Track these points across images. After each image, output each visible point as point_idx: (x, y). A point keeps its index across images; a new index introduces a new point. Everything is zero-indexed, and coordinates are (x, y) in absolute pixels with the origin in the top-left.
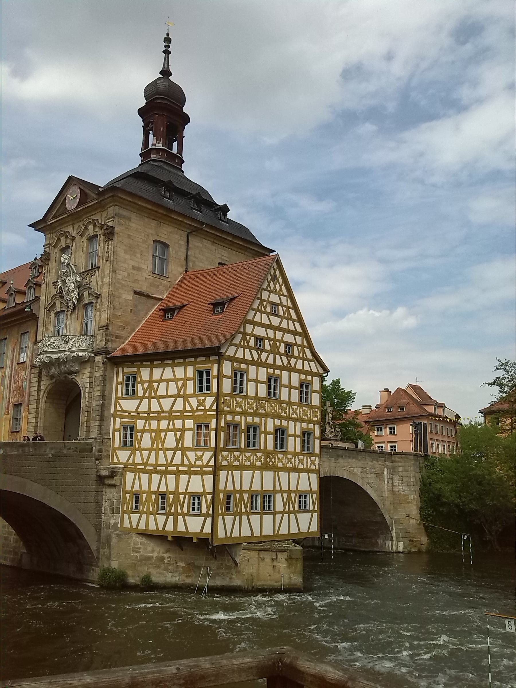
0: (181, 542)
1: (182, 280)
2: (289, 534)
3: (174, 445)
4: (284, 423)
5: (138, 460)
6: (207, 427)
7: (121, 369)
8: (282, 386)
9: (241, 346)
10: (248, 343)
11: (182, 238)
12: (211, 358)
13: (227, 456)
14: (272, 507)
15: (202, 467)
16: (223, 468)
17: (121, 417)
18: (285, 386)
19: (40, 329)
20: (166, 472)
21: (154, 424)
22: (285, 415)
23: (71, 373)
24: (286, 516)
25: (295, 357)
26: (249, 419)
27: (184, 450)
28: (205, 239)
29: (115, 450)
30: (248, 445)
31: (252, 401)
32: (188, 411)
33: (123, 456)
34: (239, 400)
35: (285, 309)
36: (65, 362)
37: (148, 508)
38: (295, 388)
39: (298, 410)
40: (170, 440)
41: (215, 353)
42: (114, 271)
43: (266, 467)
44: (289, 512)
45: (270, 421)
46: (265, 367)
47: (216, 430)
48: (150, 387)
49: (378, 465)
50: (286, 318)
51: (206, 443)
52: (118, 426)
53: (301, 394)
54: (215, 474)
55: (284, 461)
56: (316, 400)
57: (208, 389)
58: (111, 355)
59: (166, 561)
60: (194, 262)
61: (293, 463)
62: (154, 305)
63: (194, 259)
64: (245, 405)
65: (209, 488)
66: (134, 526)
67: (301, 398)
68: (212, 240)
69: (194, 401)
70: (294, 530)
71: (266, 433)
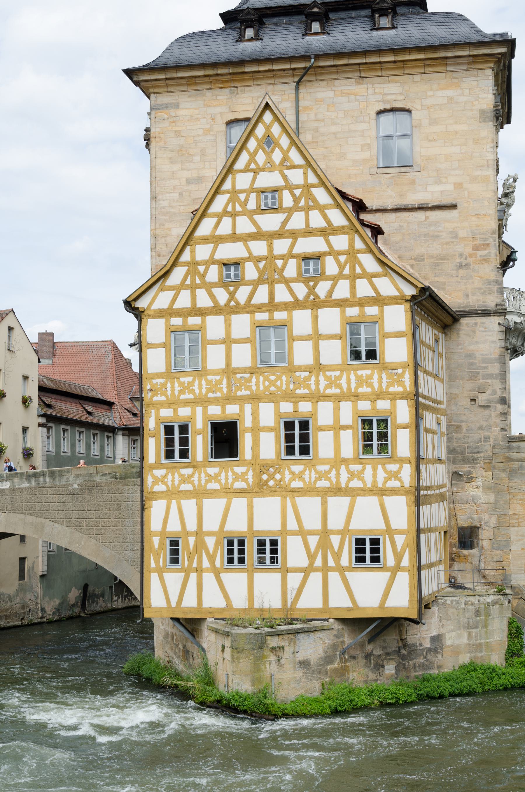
4: (305, 408)
8: (293, 339)
10: (203, 276)
11: (286, 97)
13: (166, 476)
16: (160, 495)
18: (302, 338)
22: (307, 391)
28: (338, 79)
31: (218, 377)
34: (186, 380)
35: (297, 192)
39: (344, 378)
43: (261, 488)
44: (325, 569)
46: (248, 312)
55: (306, 477)
56: (396, 351)
60: (316, 130)
61: (334, 480)
63: (315, 125)
64: (200, 387)
68: (357, 74)
70: (339, 601)
71: (256, 430)
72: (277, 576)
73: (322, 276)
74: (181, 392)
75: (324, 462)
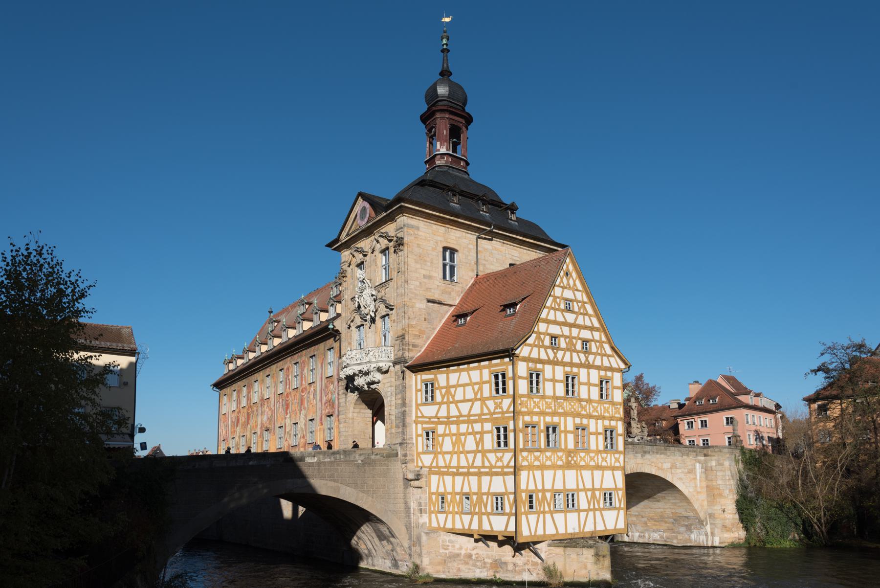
0: (487, 538)
1: (473, 285)
2: (595, 531)
3: (474, 448)
4: (585, 421)
5: (441, 463)
6: (505, 429)
7: (419, 377)
8: (580, 384)
9: (536, 346)
10: (543, 342)
12: (507, 360)
14: (576, 505)
15: (502, 467)
17: (423, 423)
19: (344, 344)
20: (468, 474)
21: (454, 428)
23: (373, 383)
24: (591, 513)
25: (593, 354)
26: (548, 419)
27: (484, 452)
29: (418, 454)
30: (548, 445)
32: (486, 414)
33: (427, 460)
34: (536, 400)
36: (367, 374)
37: (454, 508)
38: (595, 385)
40: (470, 443)
41: (508, 353)
42: (406, 282)
43: (568, 466)
44: (594, 510)
45: (570, 420)
47: (514, 431)
48: (448, 392)
49: (689, 460)
50: (581, 314)
51: (506, 444)
52: (420, 432)
53: (601, 391)
54: (515, 473)
56: (618, 396)
57: (504, 391)
58: (410, 363)
59: (474, 557)
62: (447, 312)
64: (543, 405)
65: (511, 489)
66: (442, 526)
67: (602, 395)
69: (491, 404)
70: (600, 527)
71: (566, 432)
72: (576, 514)
73: (590, 353)
74: (534, 407)
75: (593, 451)
